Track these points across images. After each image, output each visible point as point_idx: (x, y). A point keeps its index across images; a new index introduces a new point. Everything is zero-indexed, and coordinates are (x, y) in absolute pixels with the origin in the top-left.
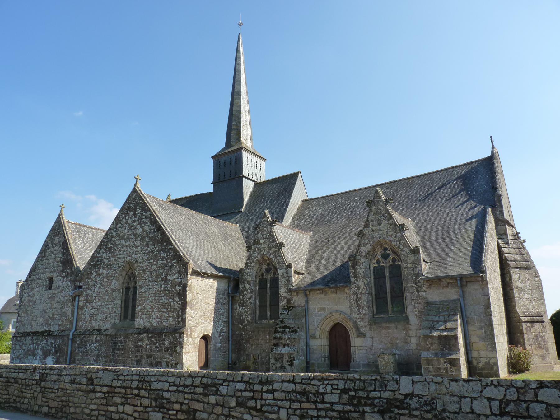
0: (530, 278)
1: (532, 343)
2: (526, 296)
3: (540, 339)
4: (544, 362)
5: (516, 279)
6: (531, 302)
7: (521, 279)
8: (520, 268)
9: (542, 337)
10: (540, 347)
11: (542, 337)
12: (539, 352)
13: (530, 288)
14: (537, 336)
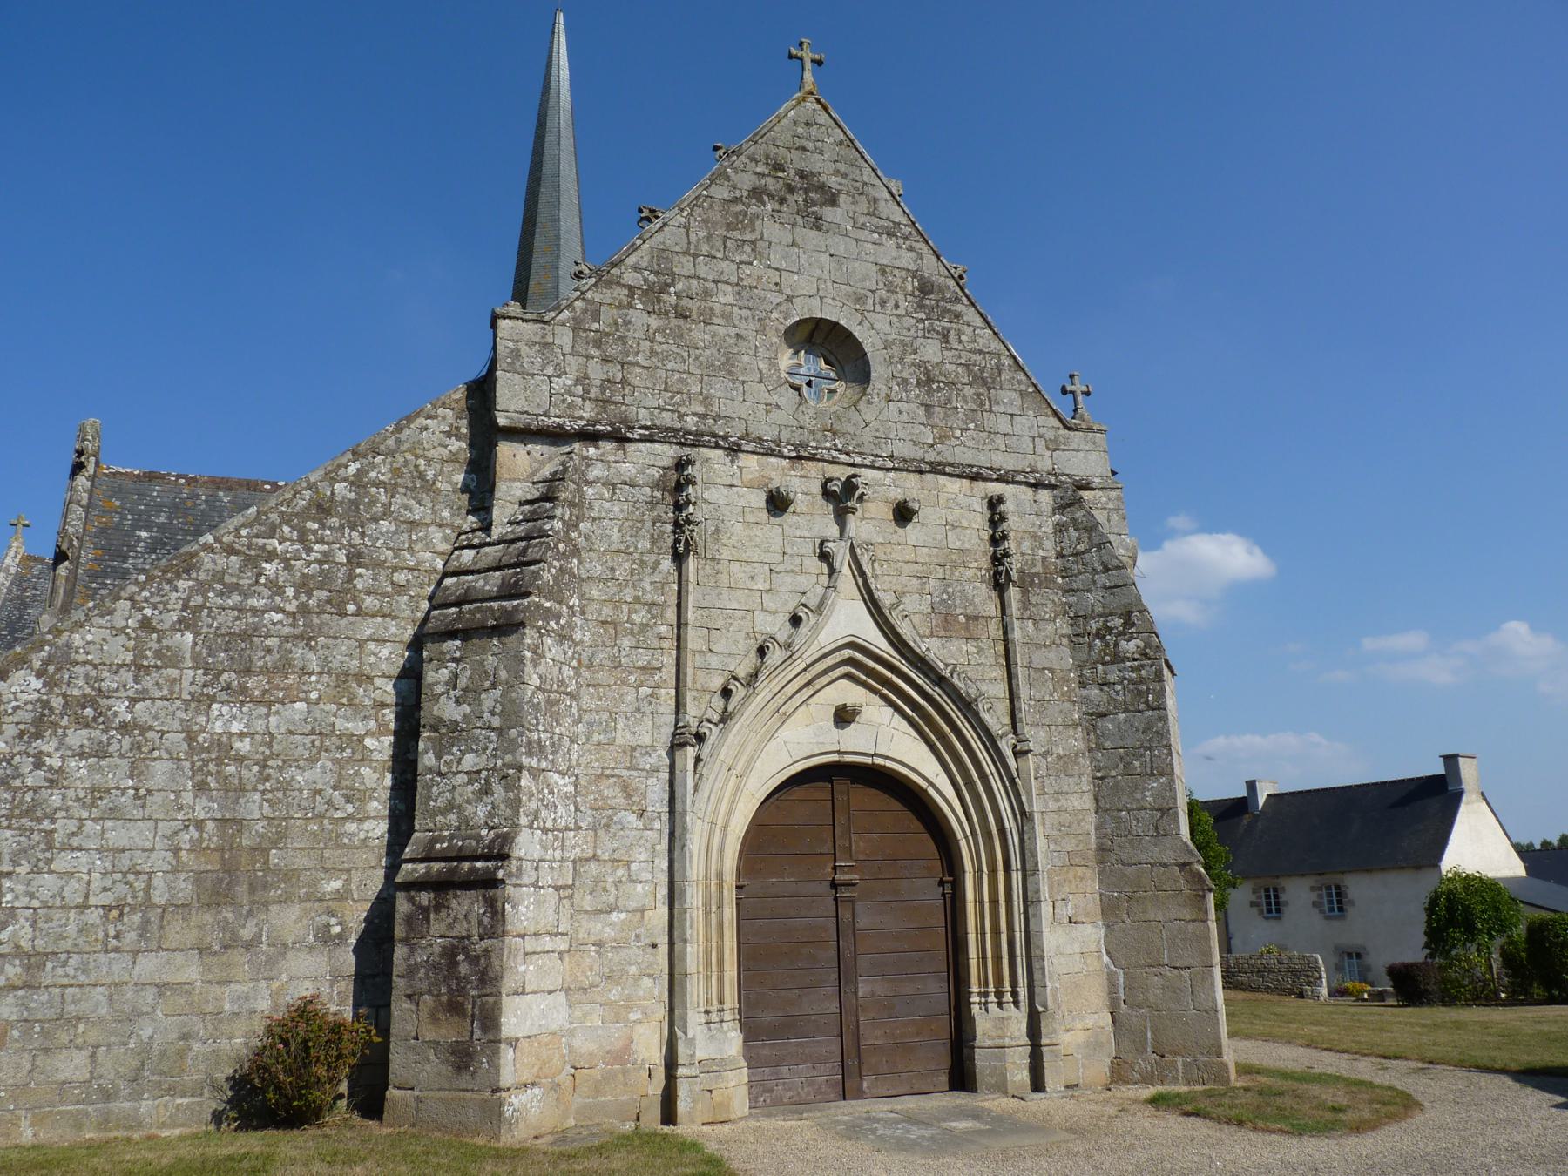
0: (503, 675)
1: (424, 986)
2: (470, 761)
3: (464, 969)
4: (464, 1080)
5: (439, 689)
6: (486, 791)
7: (463, 682)
8: (465, 634)
9: (474, 960)
10: (455, 1008)
11: (474, 960)
12: (449, 1033)
13: (496, 722)
14: (450, 954)
